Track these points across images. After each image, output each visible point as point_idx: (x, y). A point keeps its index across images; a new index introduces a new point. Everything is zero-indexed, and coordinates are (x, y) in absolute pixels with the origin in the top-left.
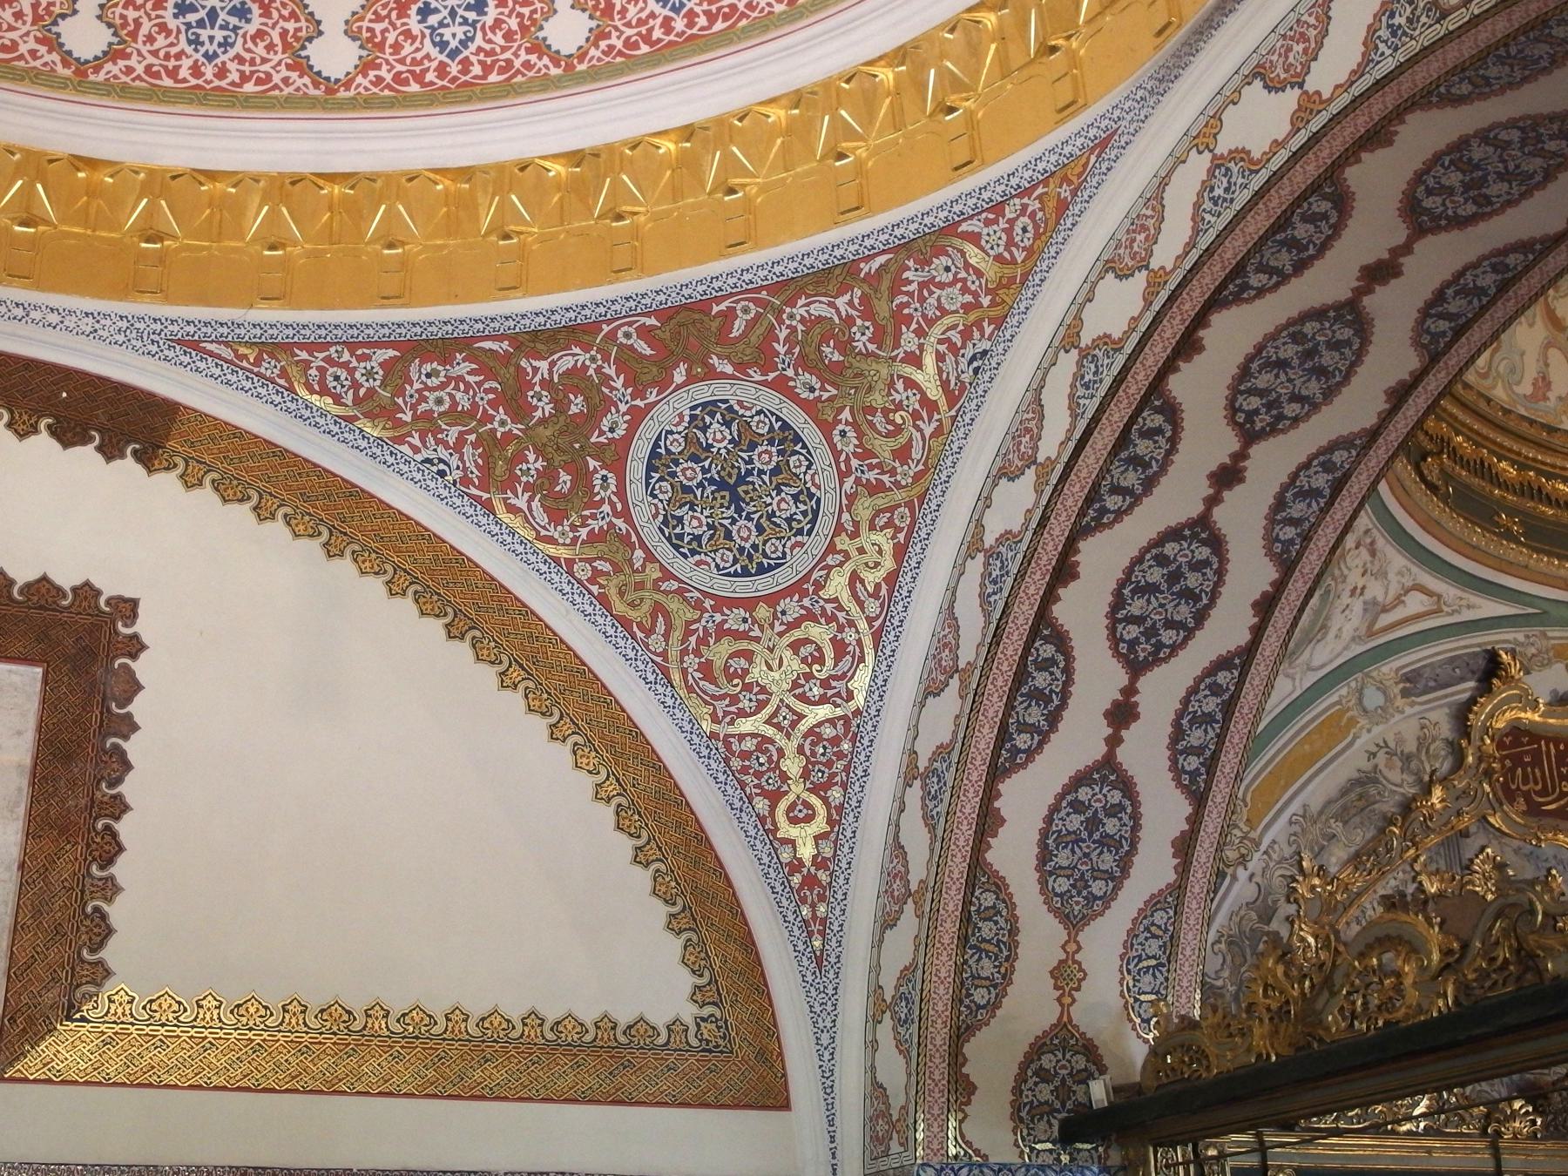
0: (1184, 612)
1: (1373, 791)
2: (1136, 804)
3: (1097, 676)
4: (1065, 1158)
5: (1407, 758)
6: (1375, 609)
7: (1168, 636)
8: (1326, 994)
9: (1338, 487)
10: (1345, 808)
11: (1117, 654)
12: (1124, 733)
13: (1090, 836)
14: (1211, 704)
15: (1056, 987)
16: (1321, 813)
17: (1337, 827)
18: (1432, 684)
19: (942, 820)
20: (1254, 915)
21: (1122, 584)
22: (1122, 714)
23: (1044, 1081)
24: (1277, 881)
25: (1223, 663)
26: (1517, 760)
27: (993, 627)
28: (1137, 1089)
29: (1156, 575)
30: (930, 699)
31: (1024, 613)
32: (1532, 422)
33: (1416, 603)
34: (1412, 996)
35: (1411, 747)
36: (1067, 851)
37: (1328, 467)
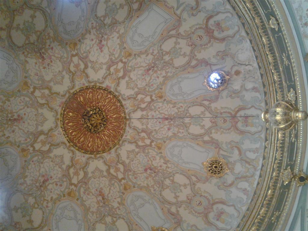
32: (252, 200)
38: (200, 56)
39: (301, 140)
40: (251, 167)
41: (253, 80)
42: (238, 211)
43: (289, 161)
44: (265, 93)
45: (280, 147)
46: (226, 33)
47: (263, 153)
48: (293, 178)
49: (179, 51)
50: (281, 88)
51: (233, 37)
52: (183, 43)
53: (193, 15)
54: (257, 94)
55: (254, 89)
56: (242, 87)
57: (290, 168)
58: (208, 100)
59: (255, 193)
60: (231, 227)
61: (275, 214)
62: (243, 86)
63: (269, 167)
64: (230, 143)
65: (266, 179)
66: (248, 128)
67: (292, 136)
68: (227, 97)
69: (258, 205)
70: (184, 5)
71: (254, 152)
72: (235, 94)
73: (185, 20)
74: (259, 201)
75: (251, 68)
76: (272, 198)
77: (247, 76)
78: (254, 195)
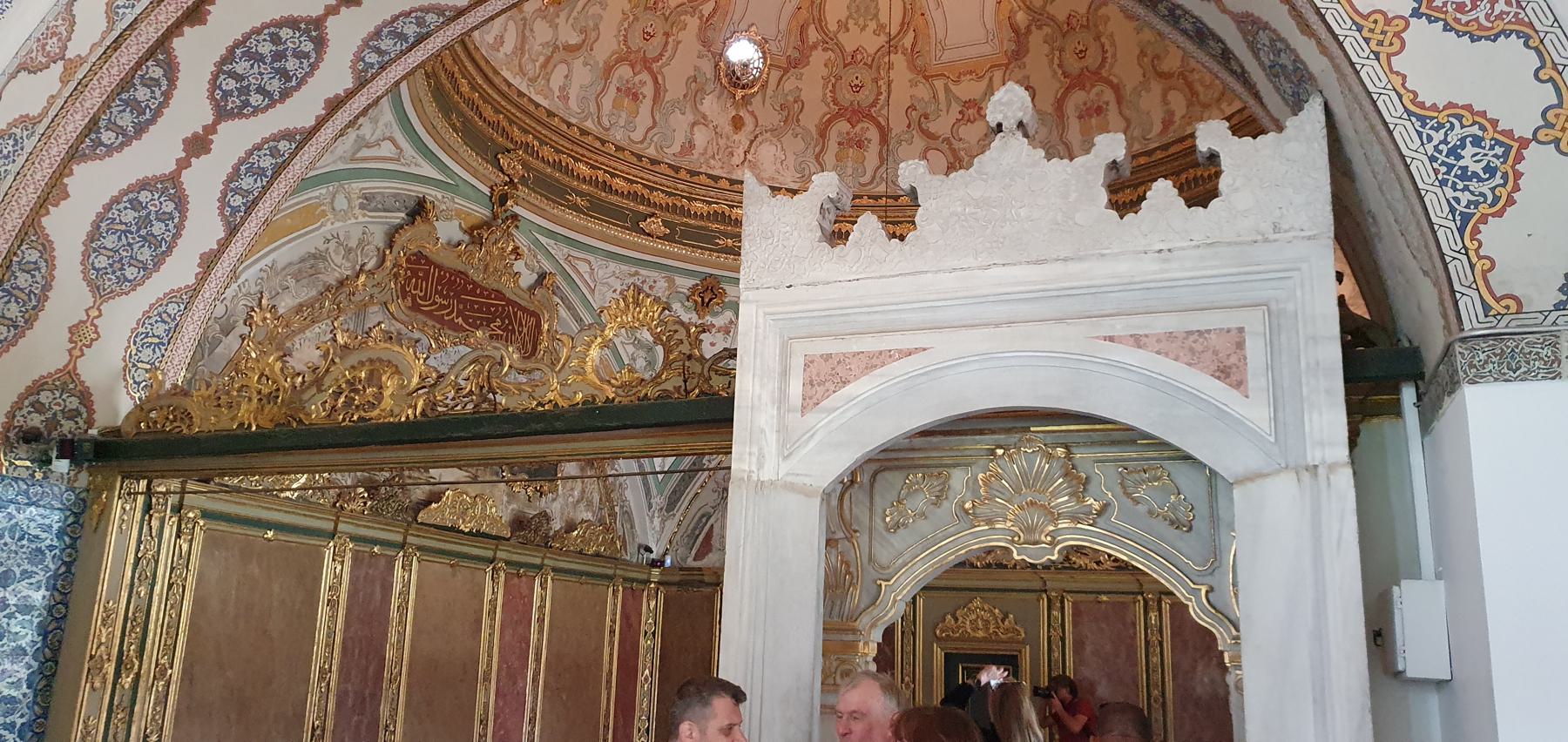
0: (275, 85)
1: (321, 265)
2: (183, 218)
3: (189, 107)
4: (38, 475)
5: (349, 251)
6: (362, 143)
7: (256, 99)
8: (314, 390)
9: (421, 39)
10: (300, 271)
11: (212, 97)
12: (193, 160)
13: (139, 230)
14: (267, 163)
15: (71, 341)
17: (291, 282)
19: (10, 178)
21: (237, 45)
22: (198, 145)
23: (37, 411)
24: (240, 307)
25: (287, 135)
26: (415, 273)
27: (115, 34)
28: (116, 431)
29: (266, 49)
30: (23, 74)
31: (149, 33)
32: (487, 62)
33: (387, 149)
34: (387, 403)
35: (353, 243)
36: (115, 237)
37: (420, 23)
38: (818, 58)
39: (570, 216)
41: (710, 153)
44: (677, 169)
46: (833, 147)
49: (861, 22)
51: (817, 158)
52: (871, 43)
53: (912, 107)
54: (676, 148)
55: (689, 146)
56: (704, 117)
58: (711, 16)
62: (702, 120)
64: (597, 27)
66: (612, 91)
68: (696, 68)
70: (943, 106)
71: (562, 89)
72: (695, 93)
73: (913, 84)
75: (736, 160)
77: (722, 142)
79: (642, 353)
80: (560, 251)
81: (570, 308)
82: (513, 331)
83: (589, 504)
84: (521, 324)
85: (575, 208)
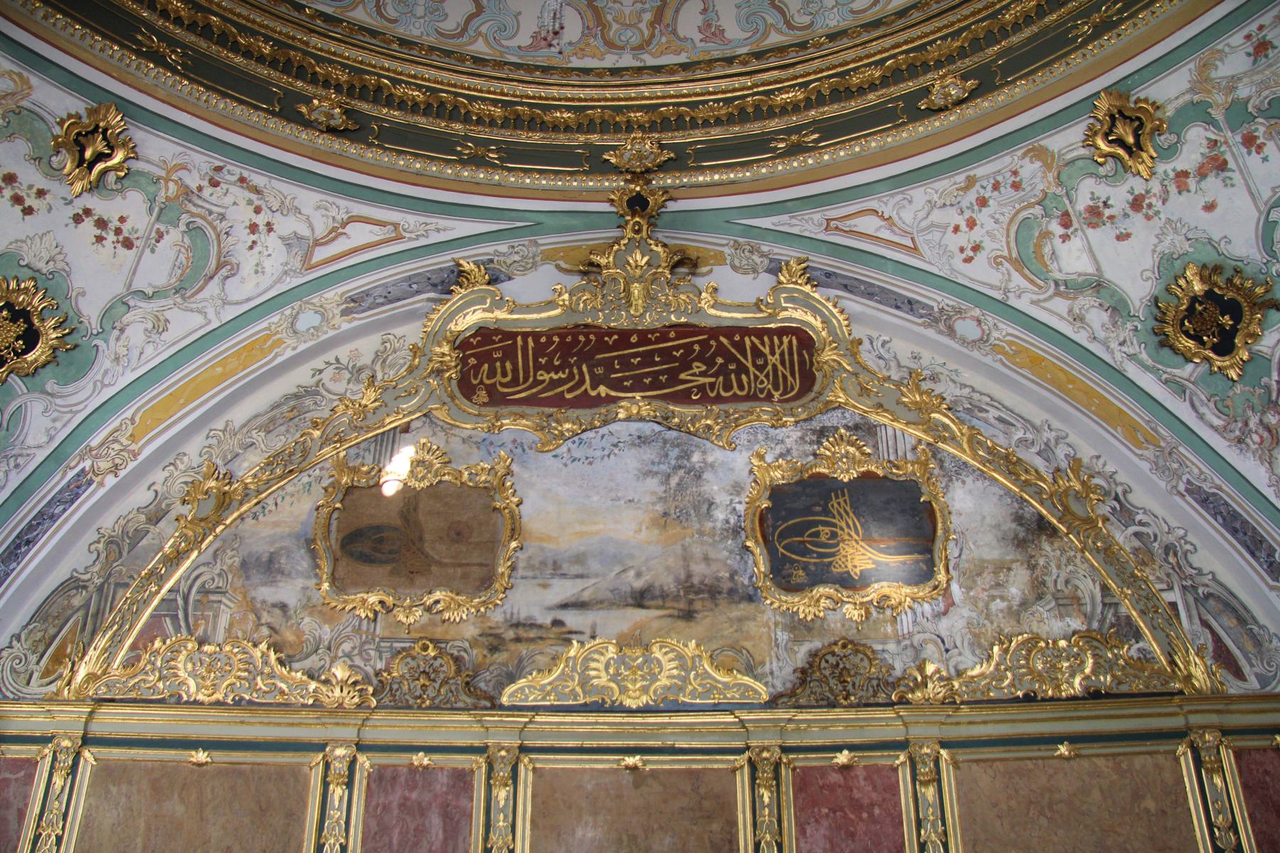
10: (272, 420)
16: (244, 426)
17: (258, 436)
18: (380, 300)
20: (143, 518)
32: (518, 66)
35: (366, 360)
40: (646, 33)
42: (465, 30)
43: (697, 151)
45: (742, 110)
47: (707, 58)
48: (634, 173)
50: (977, 45)
57: (670, 159)
59: (545, 70)
60: (395, 21)
61: (490, 151)
63: (659, 90)
65: (608, 93)
67: (794, 138)
69: (506, 87)
74: (521, 89)
76: (543, 127)
78: (537, 68)
79: (1086, 301)
80: (810, 224)
81: (871, 292)
82: (742, 369)
83: (1068, 602)
84: (757, 353)
85: (796, 150)
